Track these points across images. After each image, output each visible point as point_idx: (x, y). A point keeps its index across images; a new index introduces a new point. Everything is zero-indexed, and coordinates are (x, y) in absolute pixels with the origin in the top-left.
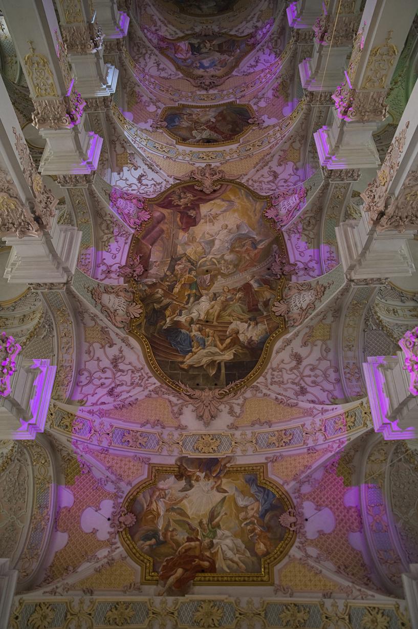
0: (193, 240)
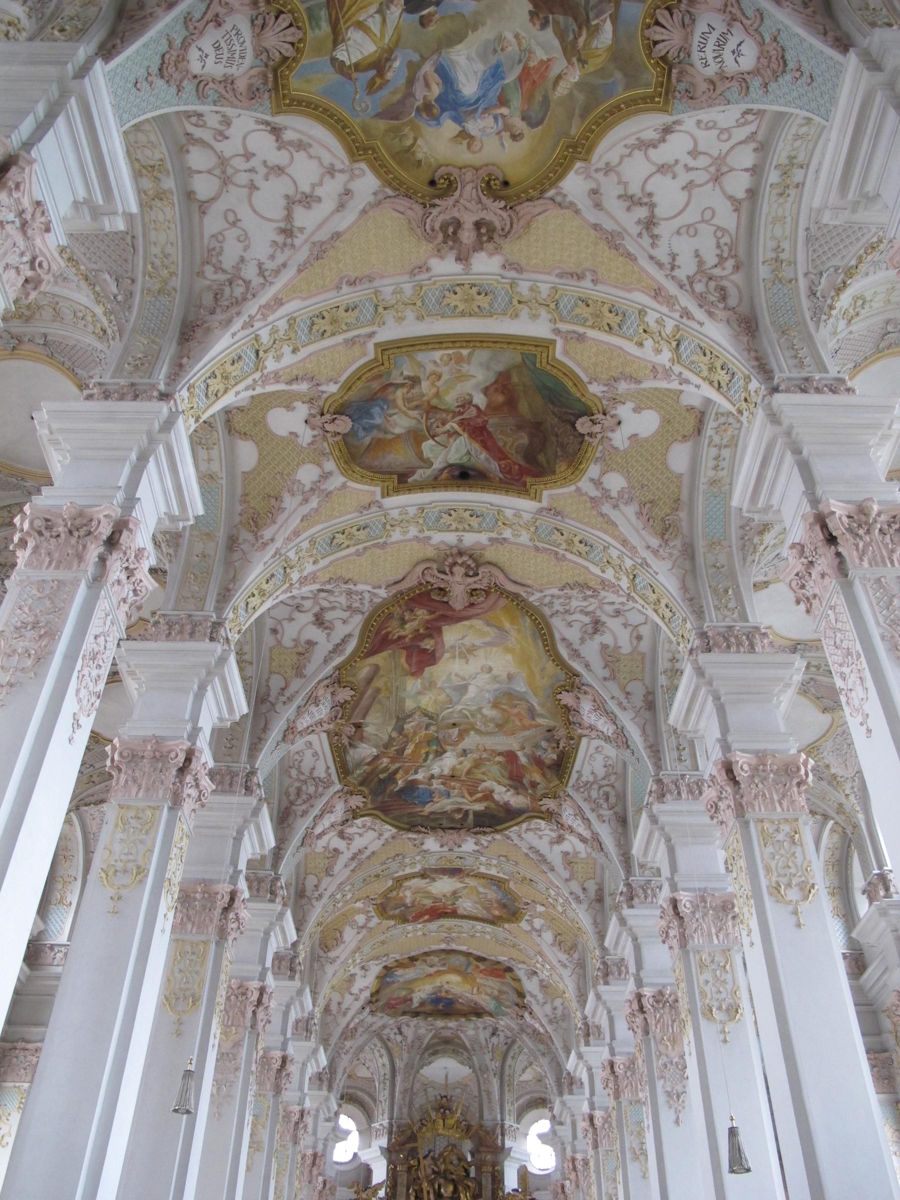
0: (431, 685)
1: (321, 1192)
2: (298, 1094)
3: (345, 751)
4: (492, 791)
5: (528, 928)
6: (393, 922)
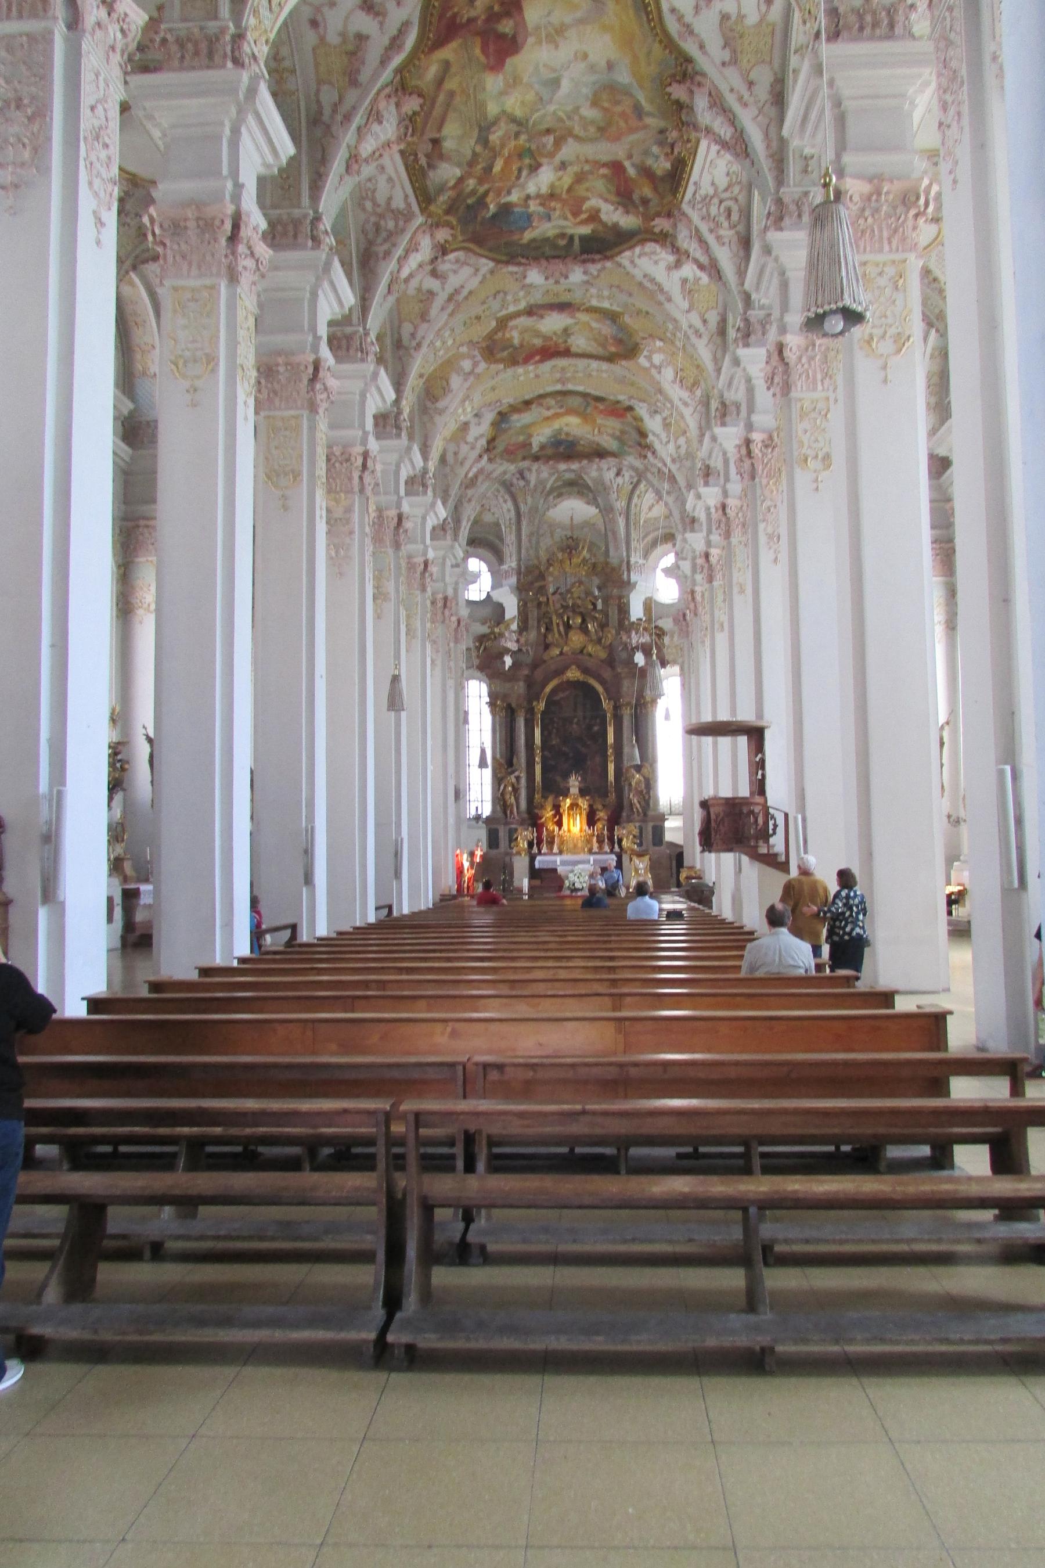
0: (515, 81)
1: (456, 630)
2: (421, 547)
3: (423, 173)
4: (598, 211)
5: (647, 364)
6: (502, 366)
